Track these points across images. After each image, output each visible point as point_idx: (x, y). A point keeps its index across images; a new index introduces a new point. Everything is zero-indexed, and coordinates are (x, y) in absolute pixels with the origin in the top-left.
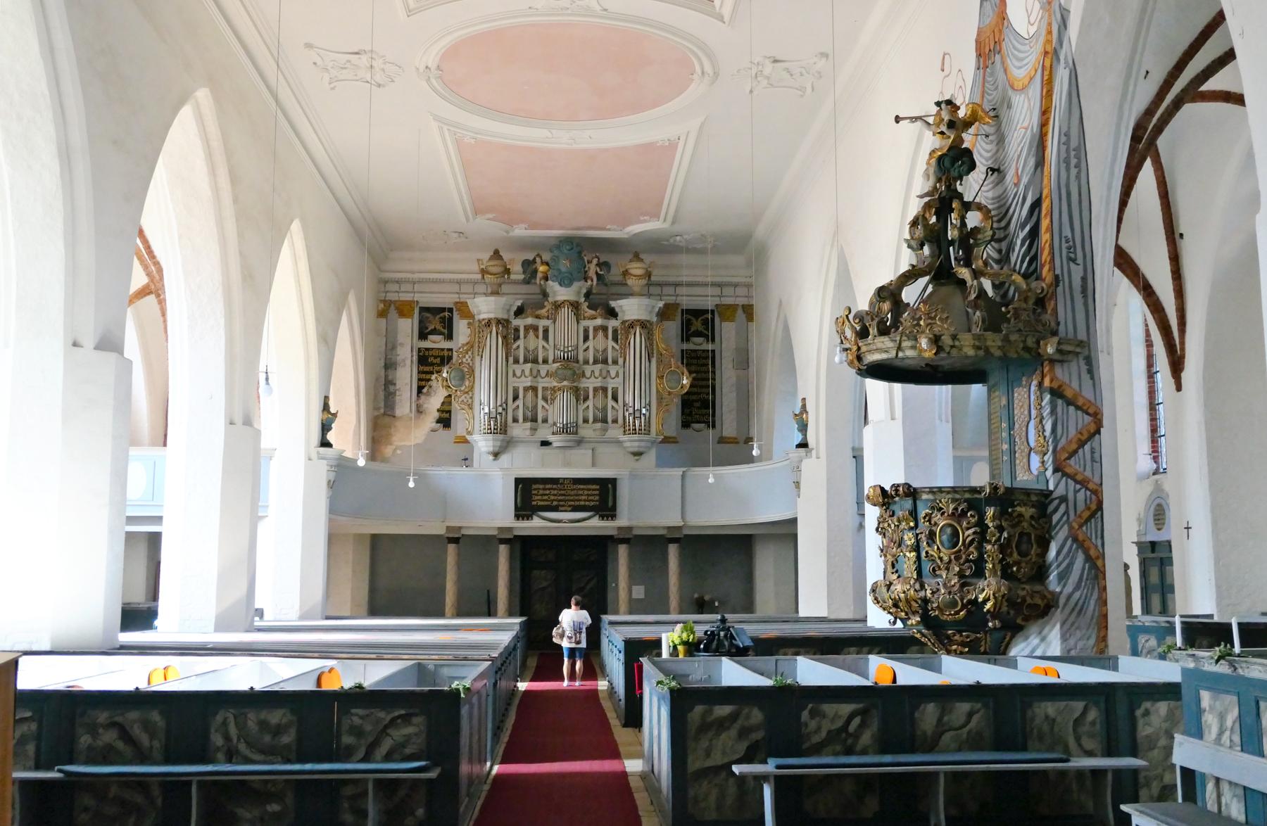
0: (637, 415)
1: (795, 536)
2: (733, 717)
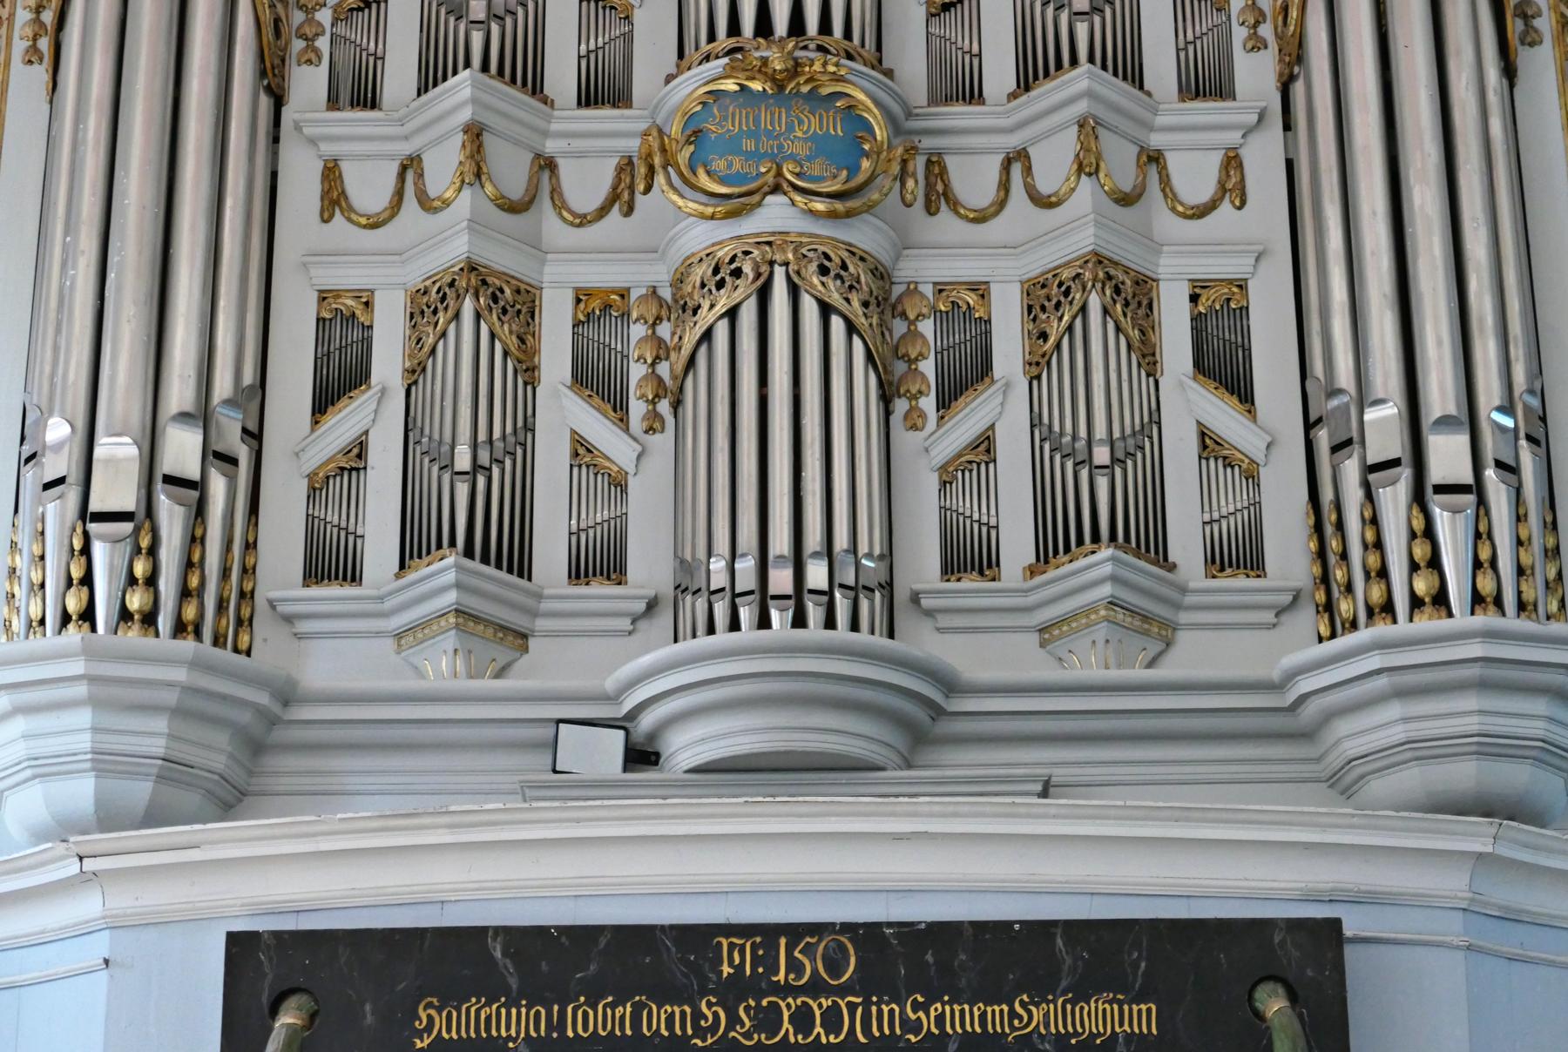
0: (1448, 457)
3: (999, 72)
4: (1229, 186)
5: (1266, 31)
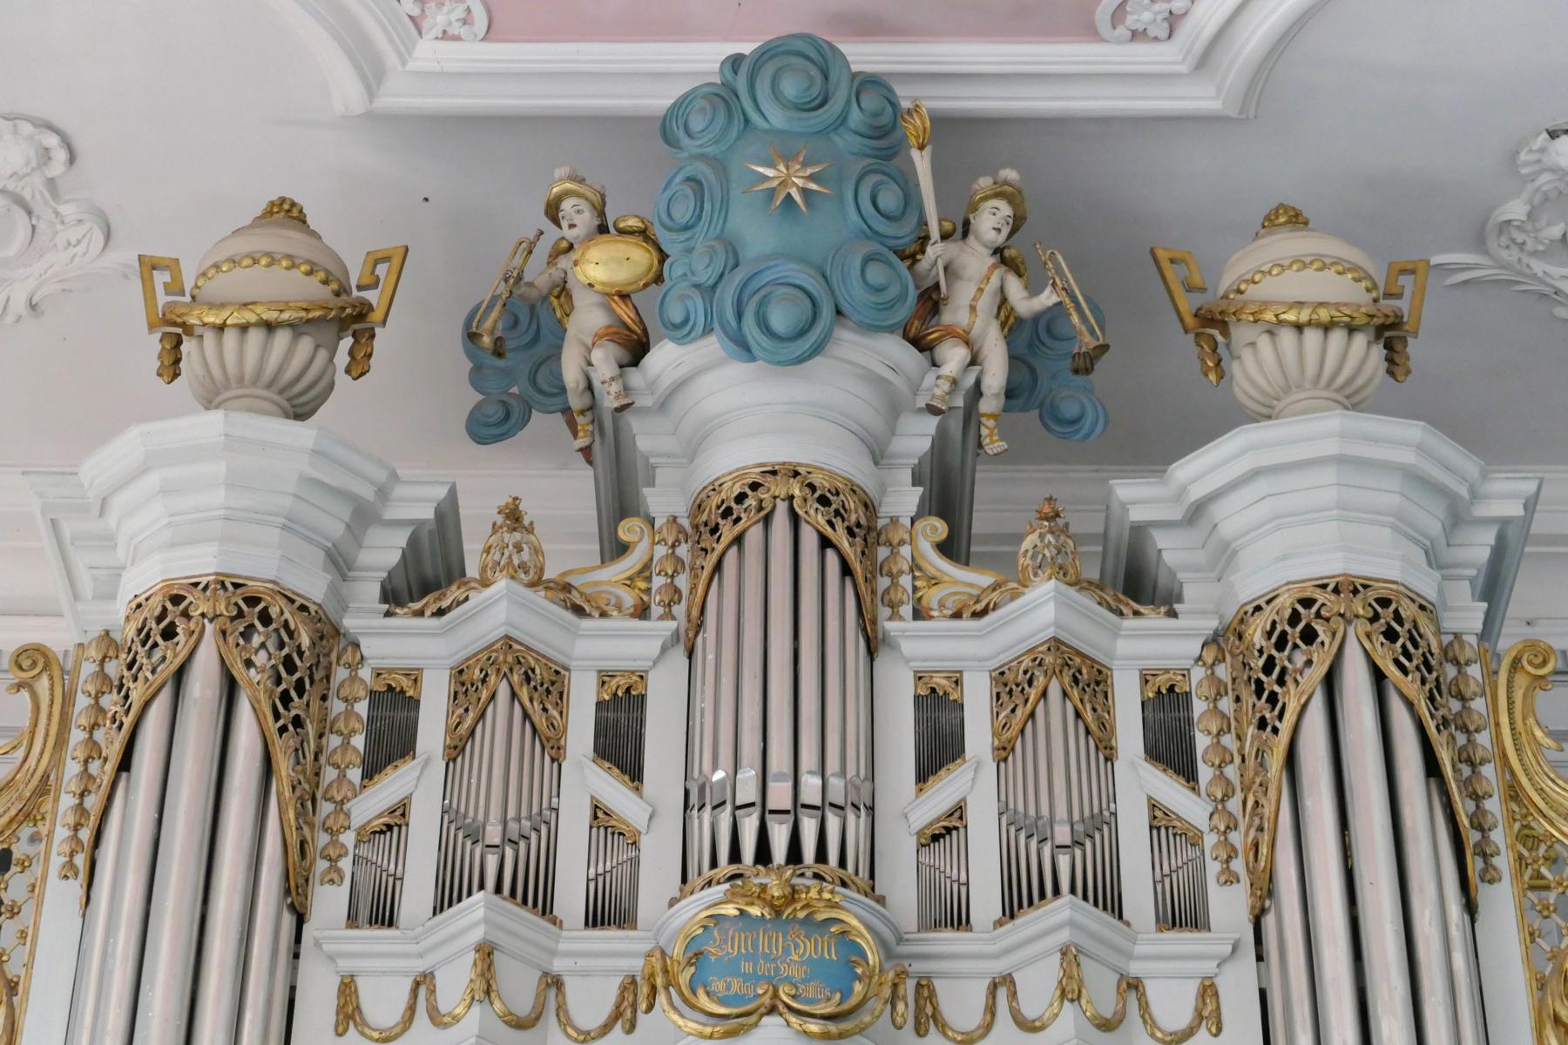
3: (986, 899)
4: (1206, 1013)
5: (1238, 865)
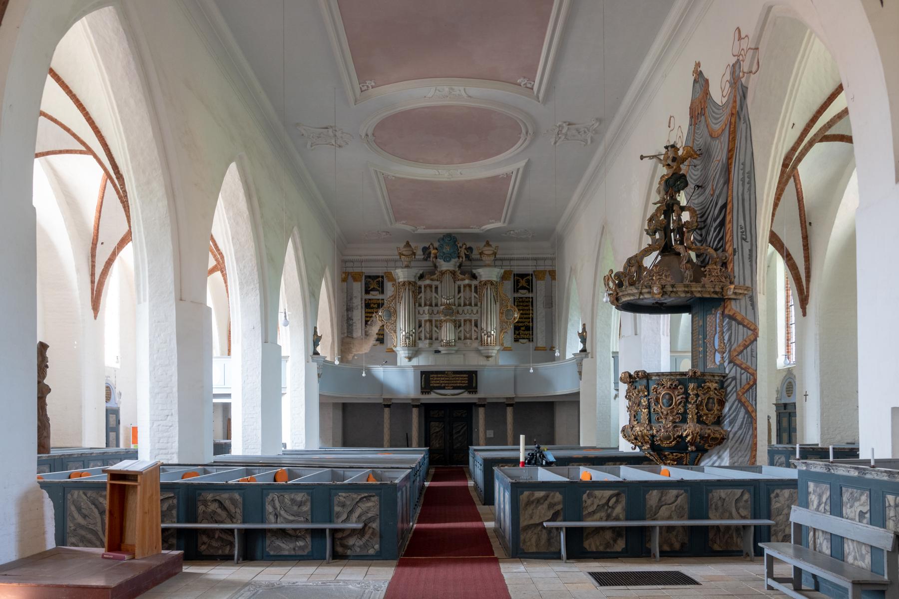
1: (578, 402)
2: (546, 498)
